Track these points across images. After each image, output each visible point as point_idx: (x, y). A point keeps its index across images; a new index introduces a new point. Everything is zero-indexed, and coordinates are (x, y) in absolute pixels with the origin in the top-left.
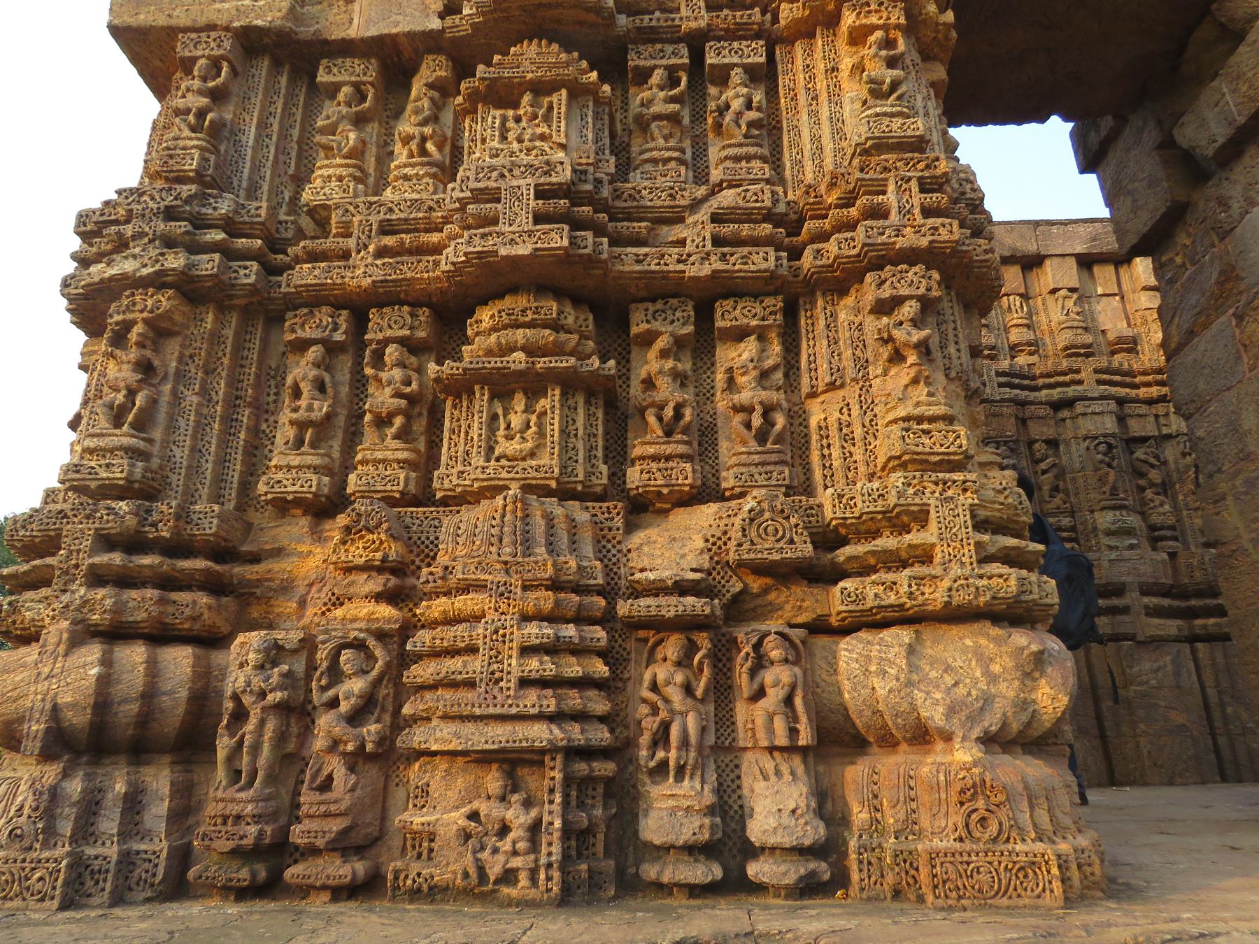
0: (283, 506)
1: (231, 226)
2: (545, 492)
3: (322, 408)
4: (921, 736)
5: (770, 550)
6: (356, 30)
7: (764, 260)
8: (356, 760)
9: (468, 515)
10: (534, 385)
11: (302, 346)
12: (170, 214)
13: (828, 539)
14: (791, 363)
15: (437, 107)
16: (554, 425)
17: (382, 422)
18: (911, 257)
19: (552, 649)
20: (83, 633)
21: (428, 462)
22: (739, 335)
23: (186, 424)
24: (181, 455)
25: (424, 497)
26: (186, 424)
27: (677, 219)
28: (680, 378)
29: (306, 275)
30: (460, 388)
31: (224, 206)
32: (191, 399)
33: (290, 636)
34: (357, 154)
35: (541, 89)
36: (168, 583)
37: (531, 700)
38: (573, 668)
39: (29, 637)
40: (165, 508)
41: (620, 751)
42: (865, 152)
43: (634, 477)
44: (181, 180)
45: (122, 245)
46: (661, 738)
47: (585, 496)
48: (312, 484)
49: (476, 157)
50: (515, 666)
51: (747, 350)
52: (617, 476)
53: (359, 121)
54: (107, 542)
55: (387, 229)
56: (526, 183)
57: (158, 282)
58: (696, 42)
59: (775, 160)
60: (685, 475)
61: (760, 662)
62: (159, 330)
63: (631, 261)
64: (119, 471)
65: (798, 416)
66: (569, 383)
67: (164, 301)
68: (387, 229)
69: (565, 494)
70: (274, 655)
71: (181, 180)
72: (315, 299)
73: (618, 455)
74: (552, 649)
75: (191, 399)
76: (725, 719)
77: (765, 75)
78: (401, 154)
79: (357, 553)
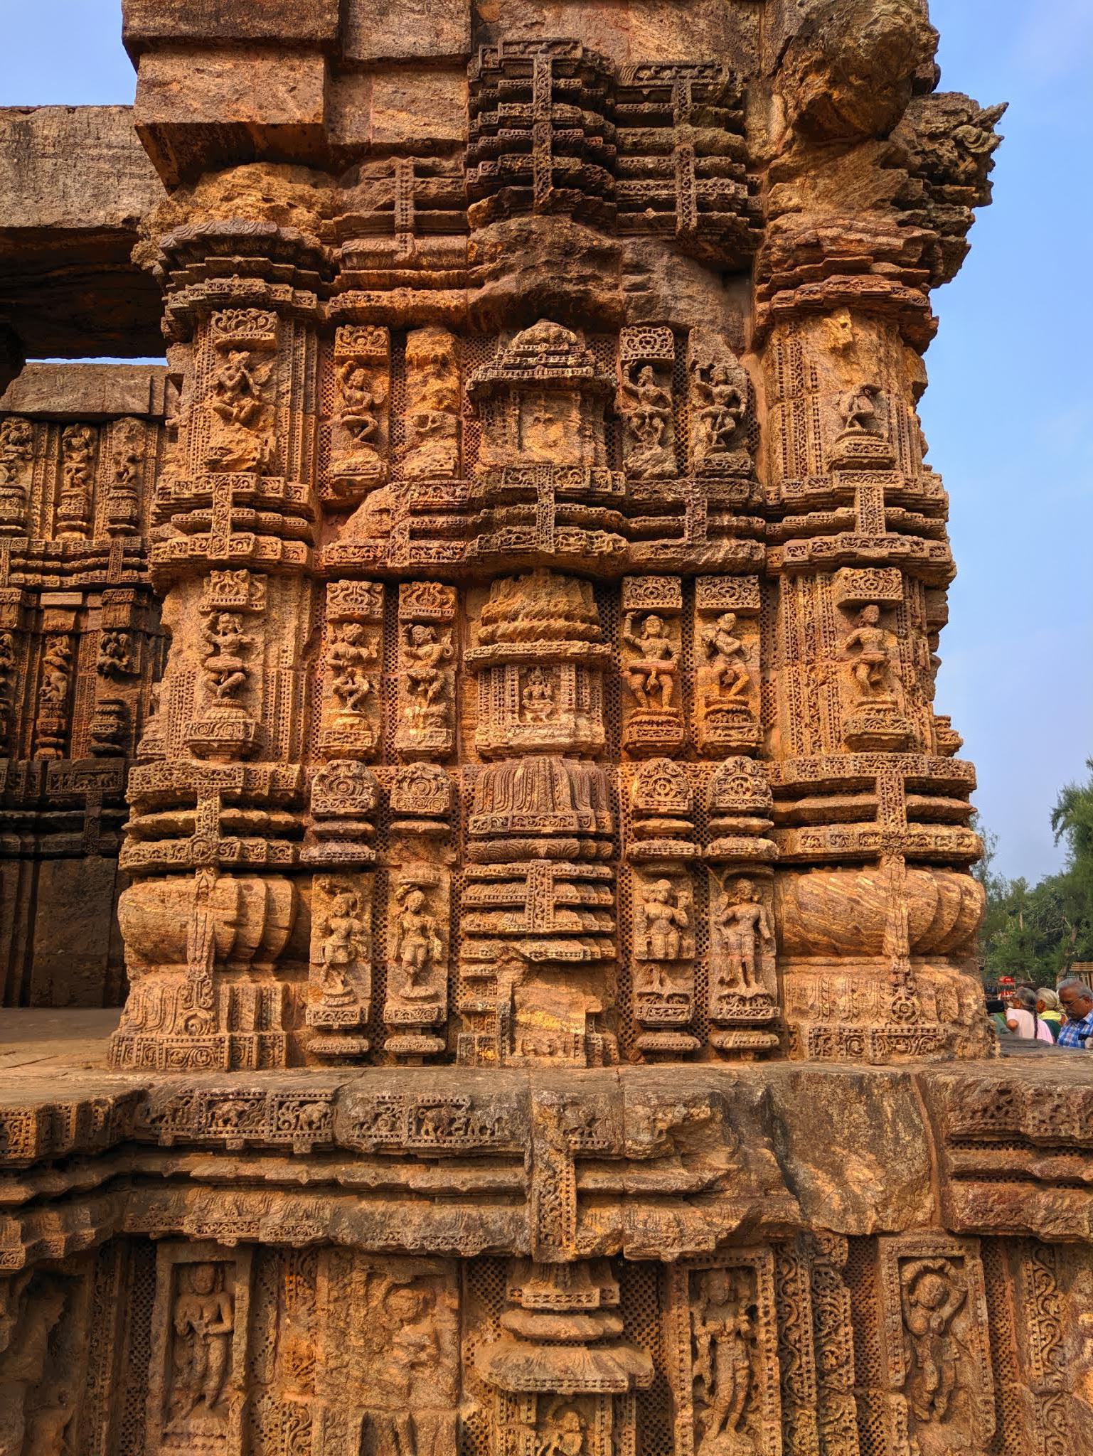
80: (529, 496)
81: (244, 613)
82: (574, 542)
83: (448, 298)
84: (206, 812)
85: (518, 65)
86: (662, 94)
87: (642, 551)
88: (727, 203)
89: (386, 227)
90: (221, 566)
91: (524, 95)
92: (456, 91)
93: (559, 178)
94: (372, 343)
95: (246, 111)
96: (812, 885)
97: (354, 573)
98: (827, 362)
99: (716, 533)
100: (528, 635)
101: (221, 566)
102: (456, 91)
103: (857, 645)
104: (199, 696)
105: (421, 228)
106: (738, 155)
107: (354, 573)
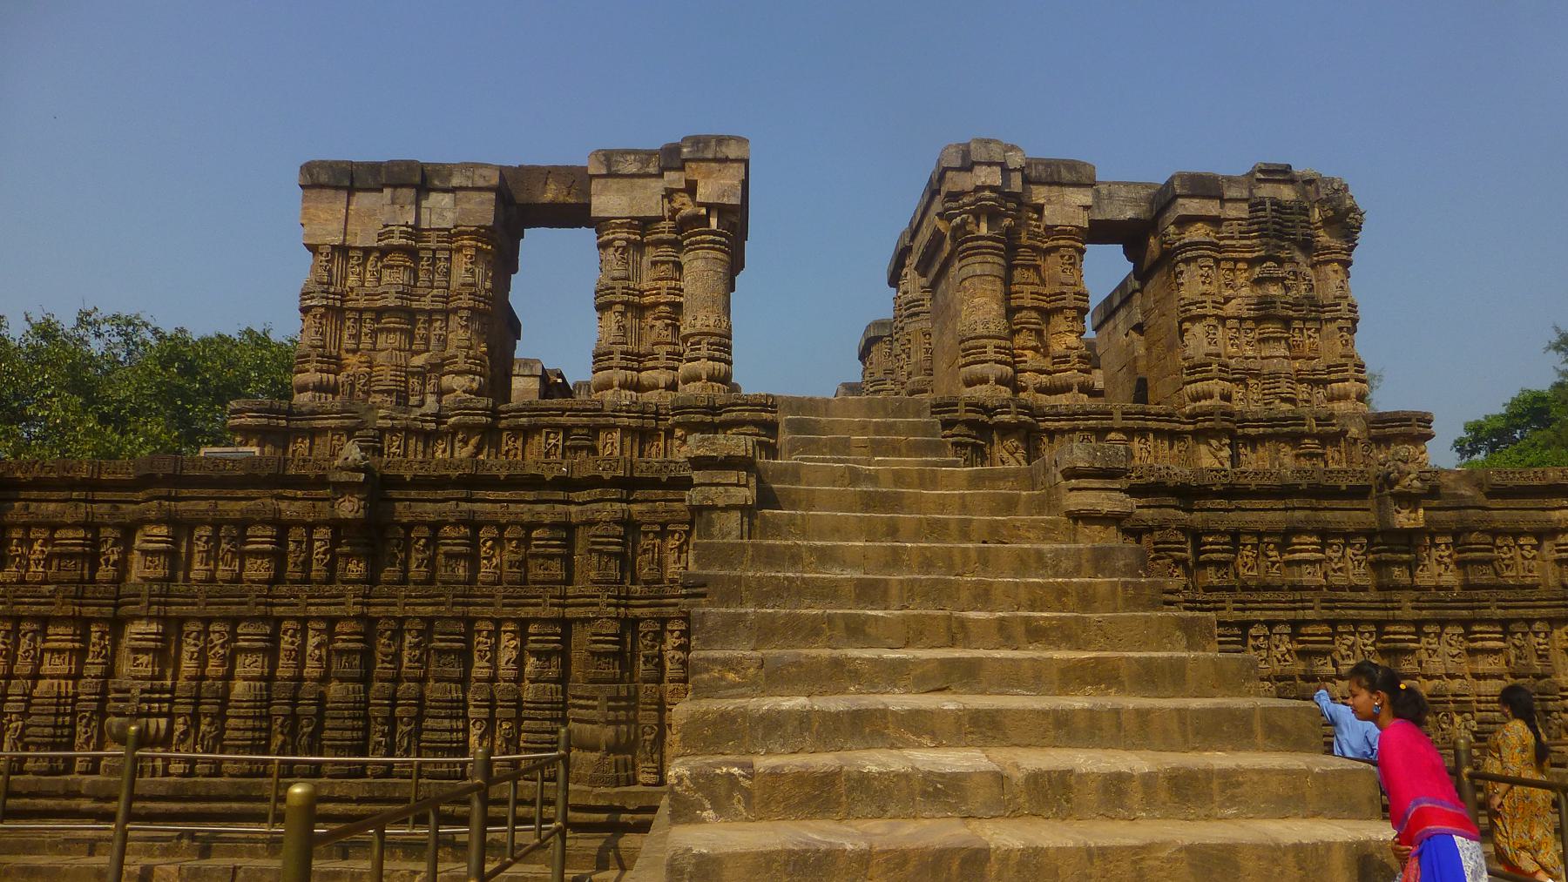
0: (347, 351)
1: (334, 293)
2: (395, 349)
3: (354, 332)
4: (455, 391)
5: (433, 361)
6: (357, 245)
7: (440, 306)
8: (364, 392)
9: (383, 353)
10: (394, 330)
11: (349, 319)
12: (323, 292)
13: (443, 360)
14: (447, 326)
15: (376, 262)
16: (398, 338)
17: (366, 335)
18: (465, 308)
19: (396, 375)
20: (316, 371)
21: (375, 343)
22: (438, 320)
23: (328, 334)
24: (328, 339)
25: (375, 350)
26: (328, 334)
27: (425, 296)
28: (425, 328)
29: (350, 304)
30: (381, 330)
31: (332, 290)
32: (328, 329)
33: (352, 373)
34: (359, 274)
35: (398, 266)
36: (329, 363)
37: (392, 383)
38: (398, 379)
39: (308, 371)
40: (327, 351)
41: (407, 393)
42: (463, 285)
43: (414, 347)
44: (324, 284)
45: (313, 298)
46: (413, 390)
47: (404, 350)
48: (354, 346)
49: (385, 279)
50: (389, 378)
51: (439, 322)
52: (410, 347)
53: (358, 265)
54: (318, 356)
55: (366, 295)
56: (393, 290)
57: (322, 306)
58: (434, 251)
59: (448, 282)
60: (422, 347)
61: (430, 379)
62: (322, 316)
63: (415, 305)
64: (319, 343)
65: (447, 336)
66: (401, 330)
67: (323, 310)
68: (366, 295)
69: (400, 350)
70: (348, 376)
71: (324, 284)
72: (351, 309)
73: (411, 344)
74: (396, 375)
75: (328, 329)
76: (425, 388)
77: (449, 260)
78: (368, 275)
79: (363, 359)
80: (1275, 302)
81: (1214, 326)
82: (1285, 313)
83: (1248, 255)
84: (1214, 367)
85: (1263, 203)
86: (1291, 208)
87: (1295, 315)
88: (1308, 235)
89: (1232, 238)
90: (1210, 316)
91: (1265, 210)
92: (1245, 206)
93: (1275, 230)
94: (1230, 265)
95: (1203, 213)
96: (1334, 385)
97: (1234, 318)
98: (1332, 274)
99: (1312, 311)
100: (1272, 332)
101: (1210, 316)
102: (1245, 206)
103: (1342, 336)
104: (1205, 344)
105: (1241, 238)
106: (1308, 222)
107: (1234, 318)
